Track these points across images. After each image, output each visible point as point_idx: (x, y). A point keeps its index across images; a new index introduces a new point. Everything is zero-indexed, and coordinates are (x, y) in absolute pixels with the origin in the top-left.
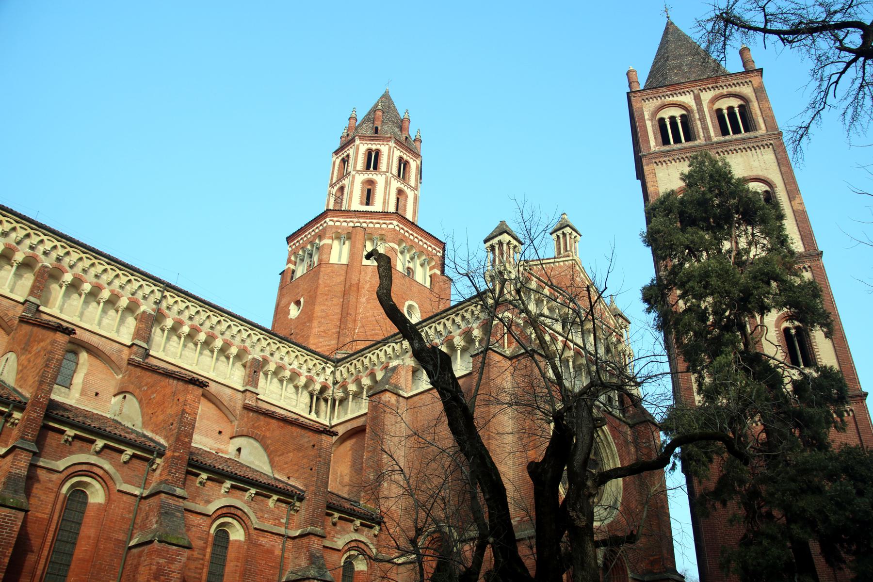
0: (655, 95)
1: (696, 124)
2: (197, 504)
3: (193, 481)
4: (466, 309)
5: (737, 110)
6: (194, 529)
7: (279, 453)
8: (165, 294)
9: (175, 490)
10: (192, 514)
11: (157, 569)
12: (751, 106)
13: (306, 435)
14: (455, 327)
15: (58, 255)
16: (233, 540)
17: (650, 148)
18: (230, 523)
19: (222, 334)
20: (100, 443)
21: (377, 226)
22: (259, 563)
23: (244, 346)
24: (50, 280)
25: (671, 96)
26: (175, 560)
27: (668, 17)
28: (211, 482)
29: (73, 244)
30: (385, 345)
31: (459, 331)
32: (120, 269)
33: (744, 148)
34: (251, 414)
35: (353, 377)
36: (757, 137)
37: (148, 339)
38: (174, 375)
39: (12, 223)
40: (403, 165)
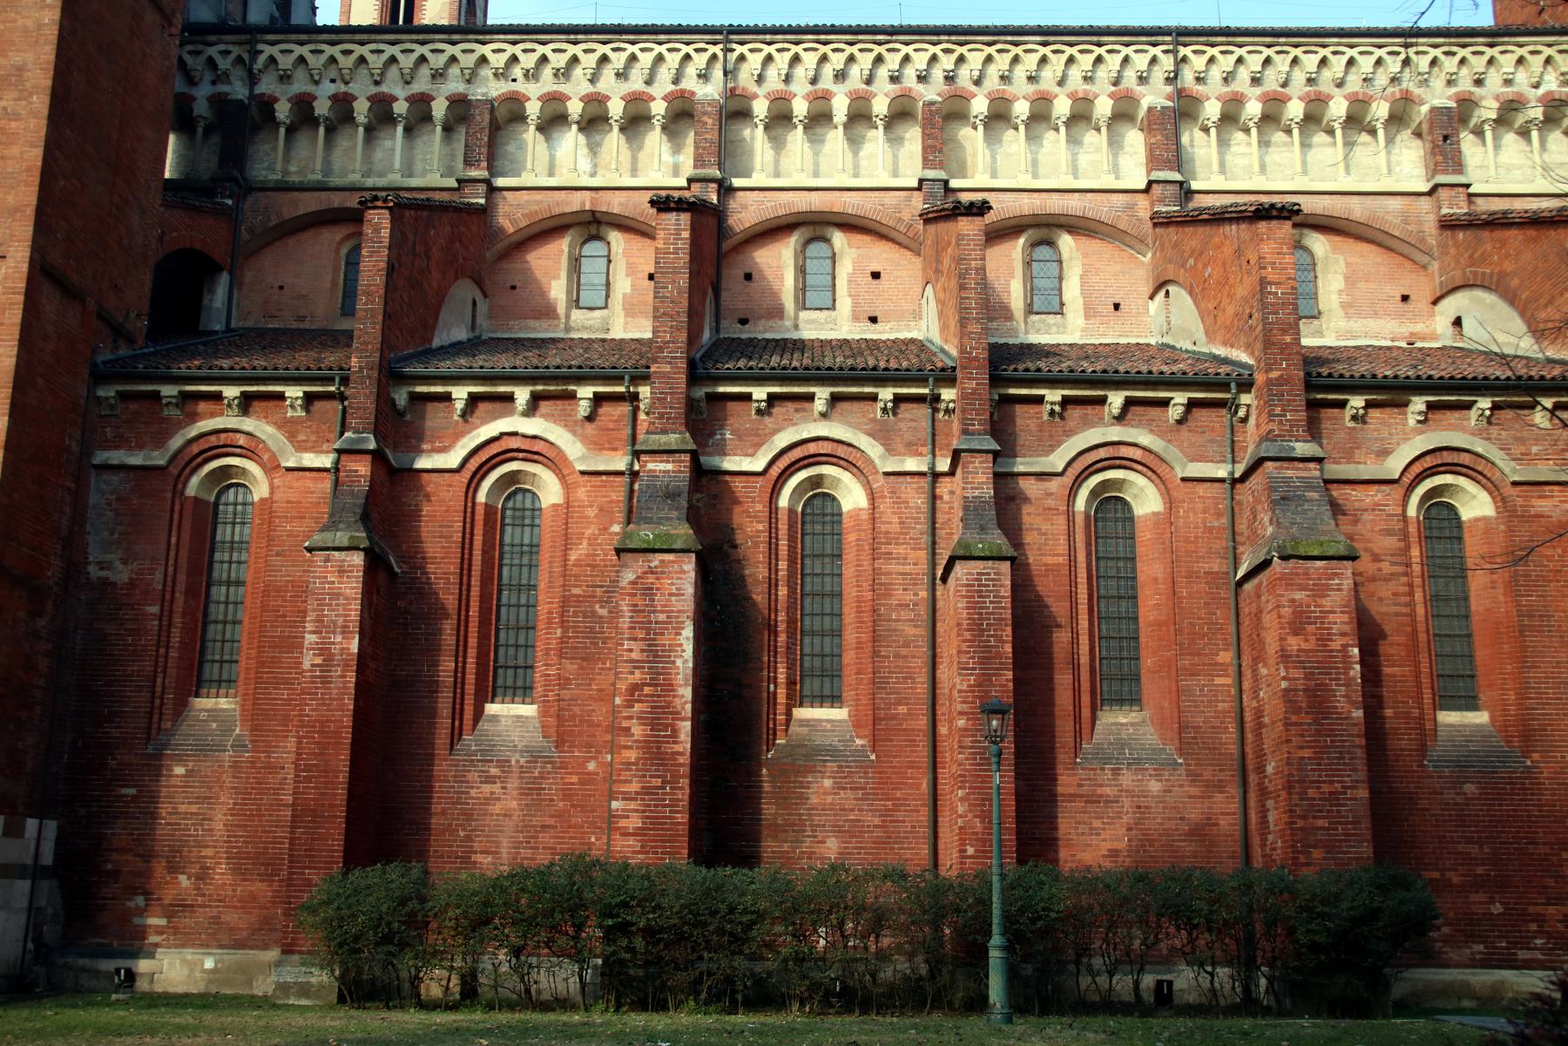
2: (1359, 463)
3: (1336, 418)
6: (1366, 517)
7: (1543, 301)
8: (1180, 55)
9: (1293, 449)
10: (1355, 486)
11: (1293, 613)
15: (945, 71)
16: (1470, 521)
18: (1452, 485)
19: (1340, 84)
20: (1116, 399)
22: (1546, 556)
23: (1401, 90)
24: (953, 125)
26: (1328, 588)
28: (1379, 410)
29: (963, 38)
32: (1071, 45)
34: (1461, 235)
37: (1178, 159)
38: (1227, 215)
39: (843, 50)
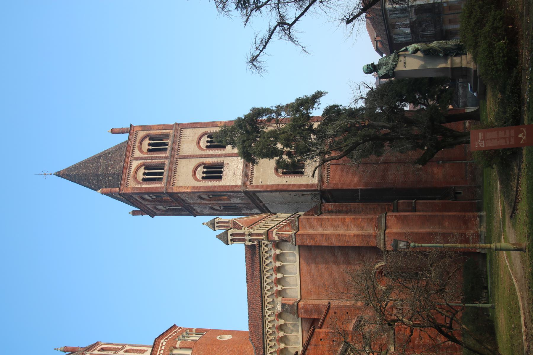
0: (126, 179)
1: (154, 162)
4: (263, 256)
5: (151, 142)
12: (152, 134)
13: (328, 320)
14: (270, 265)
17: (162, 187)
21: (162, 352)
25: (130, 172)
27: (51, 174)
30: (265, 316)
31: (273, 263)
33: (179, 142)
35: (276, 344)
36: (175, 134)
40: (103, 349)
